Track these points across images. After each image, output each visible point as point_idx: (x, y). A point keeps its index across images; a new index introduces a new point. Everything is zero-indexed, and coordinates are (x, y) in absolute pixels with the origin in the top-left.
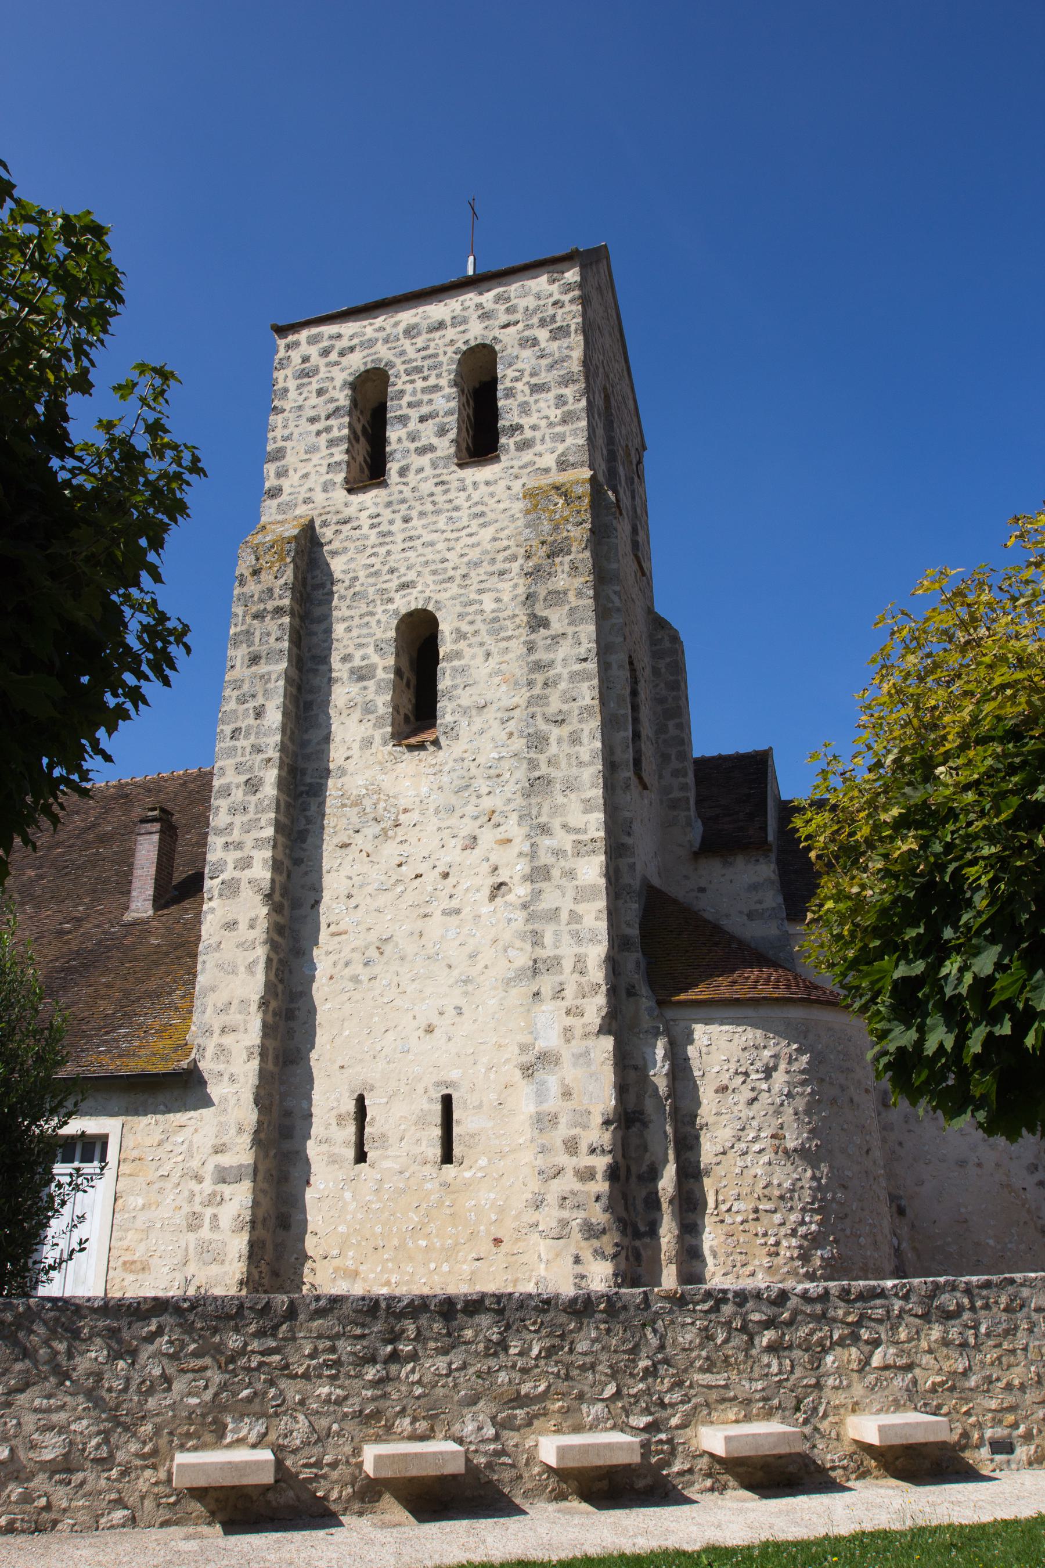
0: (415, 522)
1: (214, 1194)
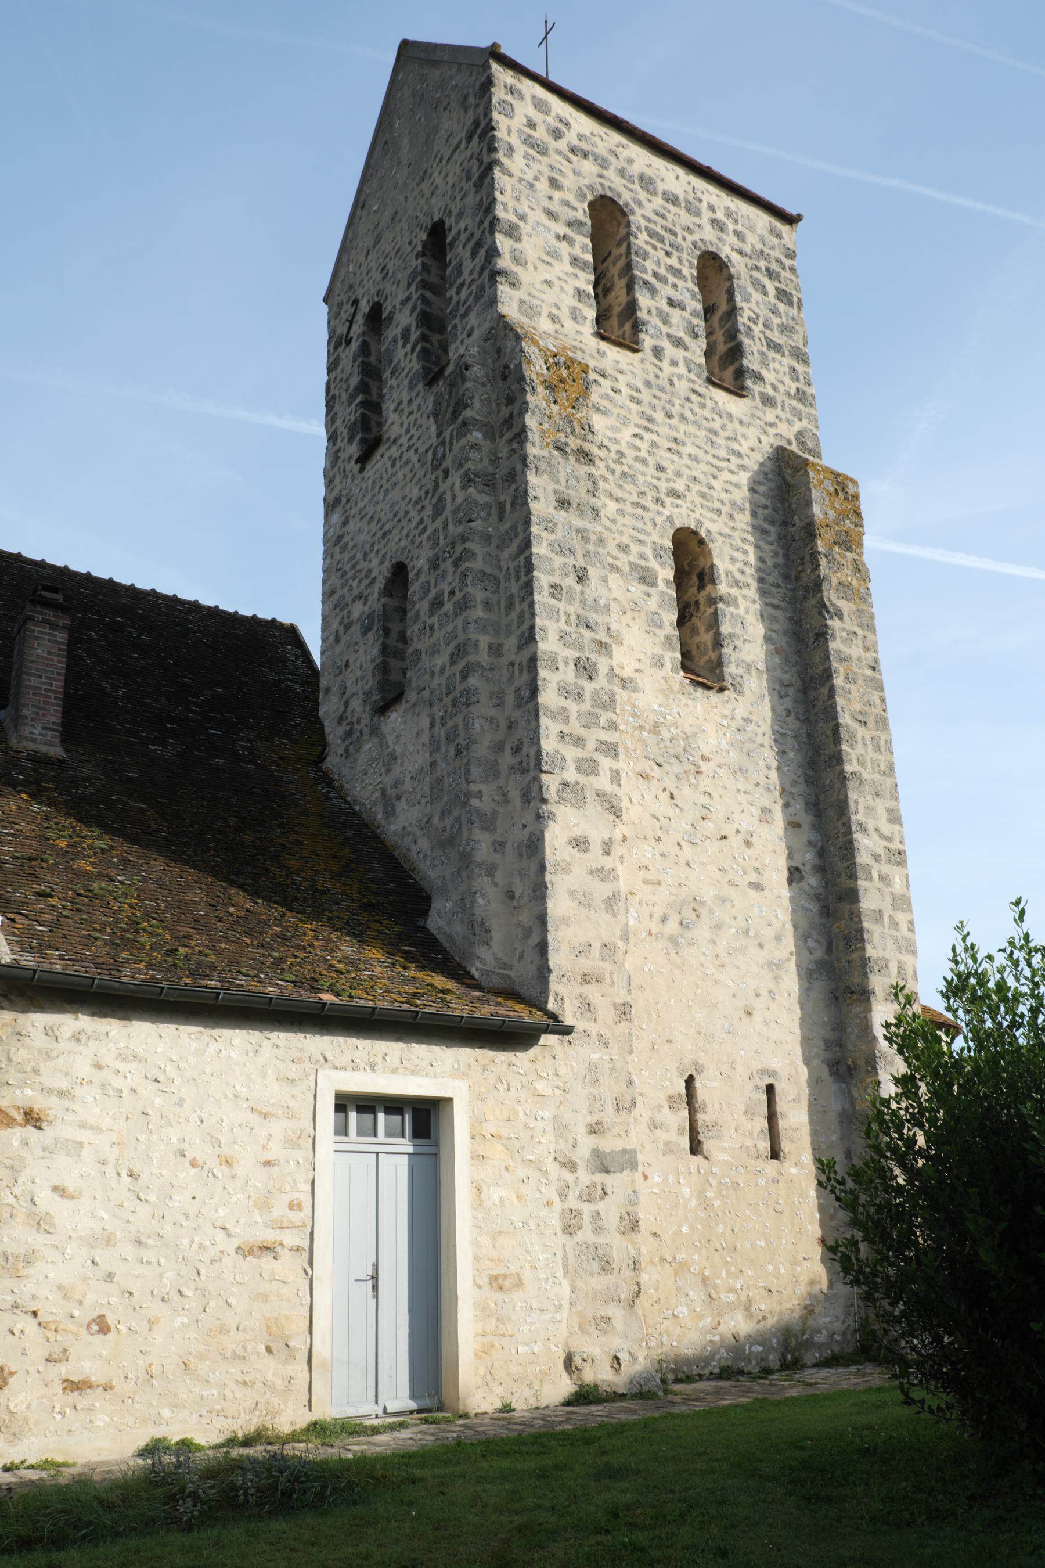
0: (674, 422)
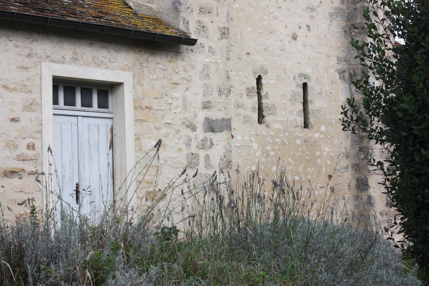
1: (204, 140)
